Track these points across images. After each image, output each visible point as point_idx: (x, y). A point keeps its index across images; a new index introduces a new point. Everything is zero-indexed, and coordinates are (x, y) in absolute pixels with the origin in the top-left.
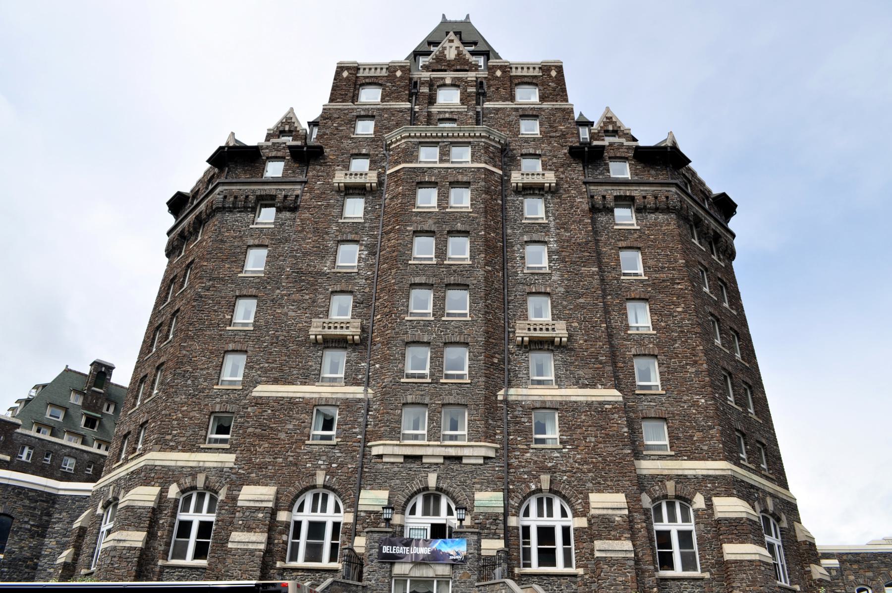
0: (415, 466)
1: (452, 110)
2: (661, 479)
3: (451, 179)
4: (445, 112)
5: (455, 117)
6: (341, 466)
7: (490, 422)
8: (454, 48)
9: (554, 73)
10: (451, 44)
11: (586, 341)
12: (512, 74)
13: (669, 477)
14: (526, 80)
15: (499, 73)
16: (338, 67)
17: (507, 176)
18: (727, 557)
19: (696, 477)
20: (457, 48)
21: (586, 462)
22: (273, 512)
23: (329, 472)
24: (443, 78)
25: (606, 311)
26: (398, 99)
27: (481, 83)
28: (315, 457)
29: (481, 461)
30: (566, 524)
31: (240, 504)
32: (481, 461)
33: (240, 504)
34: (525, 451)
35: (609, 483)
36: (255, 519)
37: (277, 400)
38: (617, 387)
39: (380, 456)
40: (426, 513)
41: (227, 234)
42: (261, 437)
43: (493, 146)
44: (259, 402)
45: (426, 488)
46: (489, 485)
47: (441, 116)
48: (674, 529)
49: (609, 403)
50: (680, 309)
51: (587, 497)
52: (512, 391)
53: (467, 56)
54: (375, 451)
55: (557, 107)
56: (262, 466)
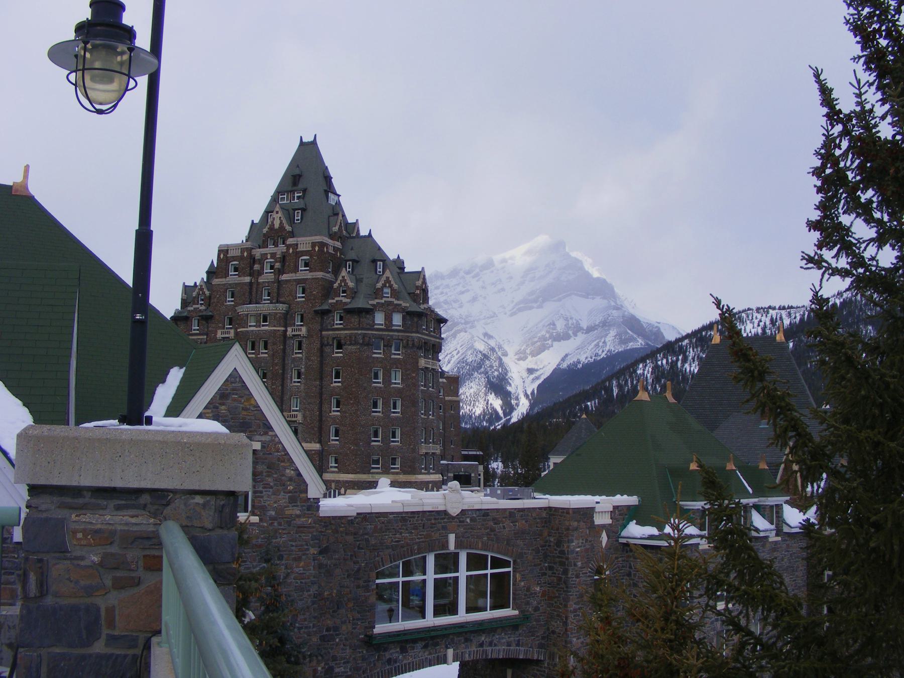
9: (317, 249)
11: (310, 420)
12: (298, 250)
13: (333, 481)
15: (291, 251)
16: (219, 251)
17: (286, 331)
19: (343, 481)
20: (280, 218)
25: (321, 404)
26: (244, 275)
38: (320, 442)
43: (280, 313)
49: (313, 450)
50: (352, 402)
55: (314, 277)
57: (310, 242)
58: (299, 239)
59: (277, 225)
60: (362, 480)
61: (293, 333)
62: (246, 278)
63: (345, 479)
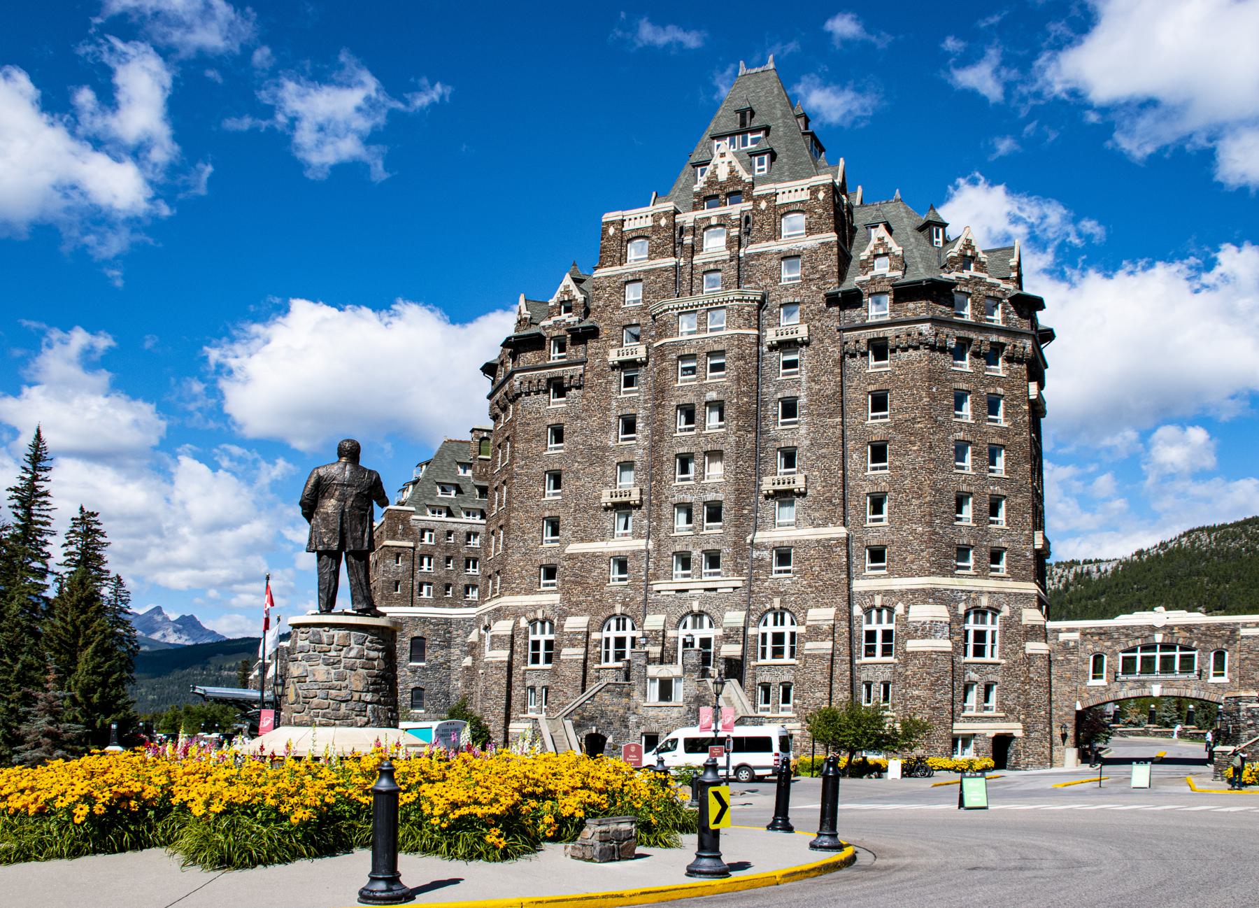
0: (684, 595)
1: (717, 259)
2: (871, 594)
3: (708, 349)
4: (710, 263)
5: (720, 267)
6: (632, 599)
7: (739, 560)
8: (726, 164)
10: (723, 159)
13: (879, 593)
14: (793, 208)
15: (763, 205)
18: (908, 650)
19: (901, 591)
21: (810, 587)
22: (588, 634)
23: (624, 604)
24: (708, 218)
27: (747, 218)
28: (613, 594)
29: (731, 590)
30: (793, 630)
31: (565, 630)
32: (731, 590)
33: (565, 630)
34: (764, 581)
35: (826, 601)
36: (576, 639)
37: (584, 555)
39: (659, 591)
40: (694, 627)
41: (528, 416)
42: (575, 583)
44: (571, 557)
45: (692, 611)
46: (736, 606)
47: (706, 268)
48: (879, 629)
51: (806, 612)
52: (758, 534)
53: (740, 173)
54: (656, 588)
56: (578, 604)
57: (805, 187)
58: (778, 186)
59: (723, 175)
60: (942, 587)
61: (780, 338)
62: (668, 260)
63: (904, 587)
